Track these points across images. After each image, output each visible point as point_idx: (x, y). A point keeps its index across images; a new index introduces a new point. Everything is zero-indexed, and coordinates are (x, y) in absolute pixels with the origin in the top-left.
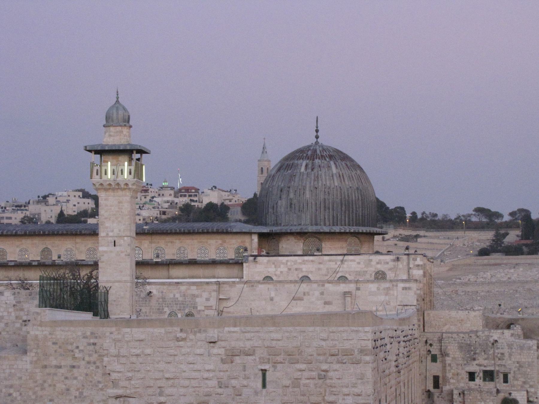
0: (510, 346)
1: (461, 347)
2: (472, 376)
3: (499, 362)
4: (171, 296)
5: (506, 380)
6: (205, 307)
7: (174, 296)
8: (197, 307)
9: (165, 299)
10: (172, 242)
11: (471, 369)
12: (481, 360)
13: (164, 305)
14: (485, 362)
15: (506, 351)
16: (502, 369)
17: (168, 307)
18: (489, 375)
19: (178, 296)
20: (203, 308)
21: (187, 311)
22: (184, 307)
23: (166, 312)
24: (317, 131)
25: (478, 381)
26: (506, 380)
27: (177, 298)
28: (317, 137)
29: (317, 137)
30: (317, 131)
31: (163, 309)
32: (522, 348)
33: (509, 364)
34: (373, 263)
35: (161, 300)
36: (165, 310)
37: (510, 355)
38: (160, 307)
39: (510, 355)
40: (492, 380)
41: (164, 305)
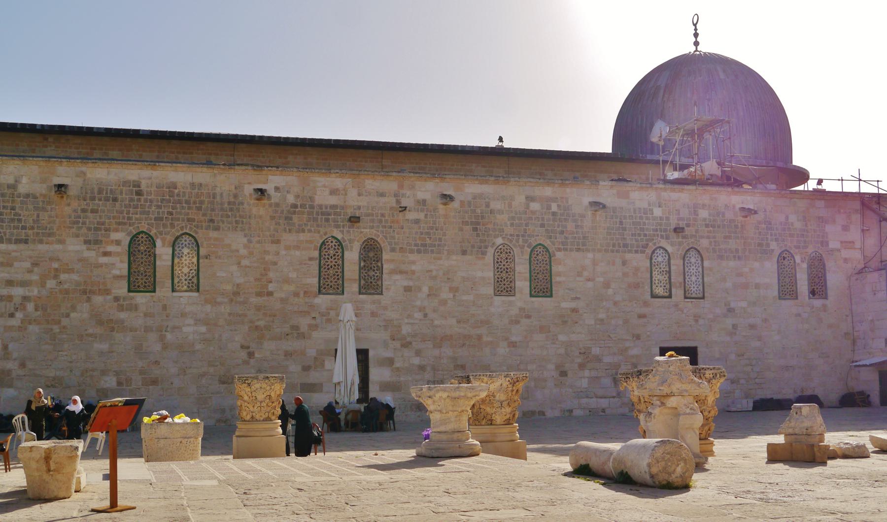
4: (782, 218)
6: (841, 242)
7: (787, 218)
8: (827, 244)
9: (770, 224)
10: (541, 174)
13: (769, 237)
17: (776, 240)
19: (793, 218)
20: (837, 245)
21: (810, 250)
22: (805, 242)
23: (773, 250)
24: (696, 35)
27: (792, 224)
28: (696, 44)
29: (696, 44)
30: (696, 35)
31: (768, 245)
35: (764, 226)
36: (772, 247)
38: (762, 240)
41: (769, 237)
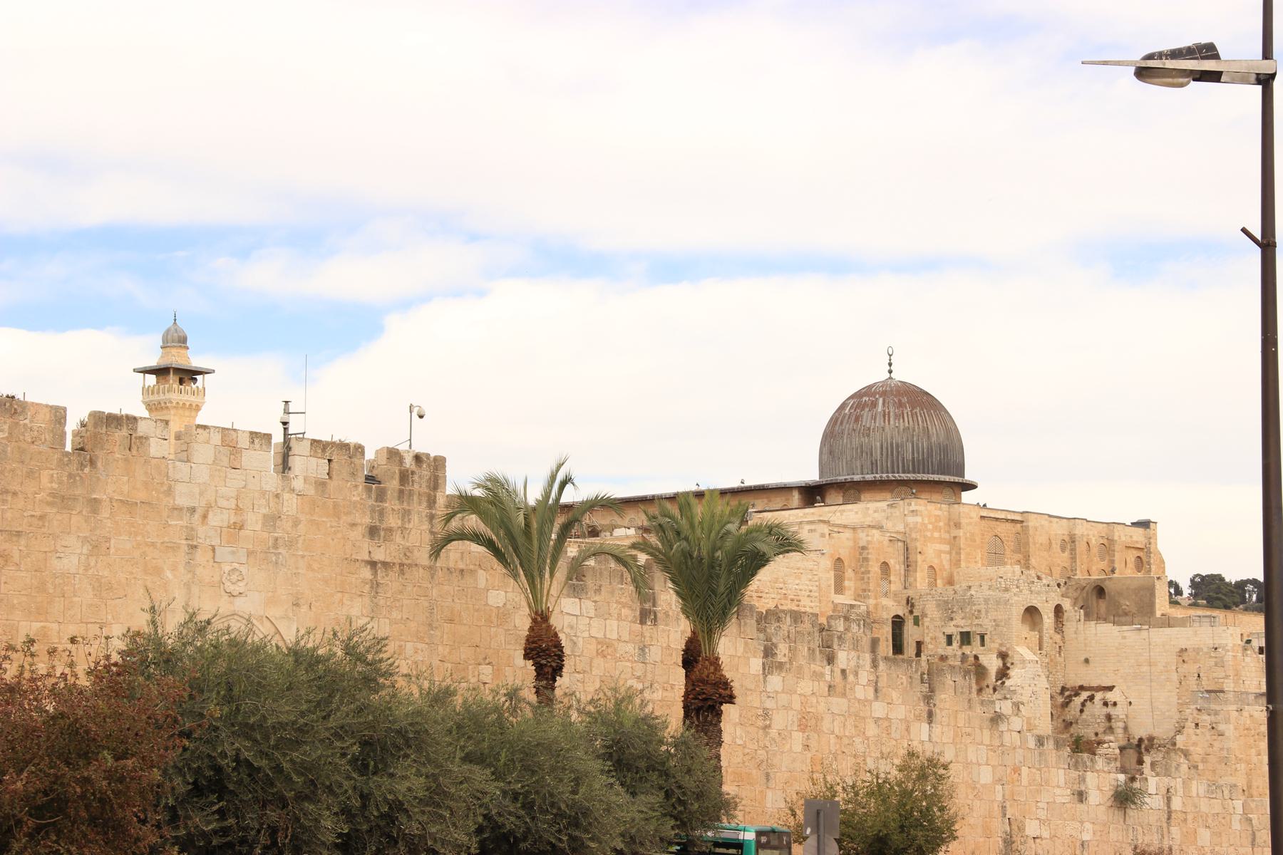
0: (986, 601)
1: (938, 606)
2: (949, 640)
3: (976, 622)
5: (983, 644)
11: (948, 631)
12: (959, 620)
14: (962, 623)
15: (982, 607)
16: (979, 630)
18: (966, 638)
24: (890, 365)
25: (955, 645)
26: (983, 644)
28: (890, 372)
29: (890, 372)
30: (890, 365)
32: (998, 603)
33: (986, 624)
34: (871, 512)
37: (987, 612)
39: (987, 612)
40: (969, 643)
